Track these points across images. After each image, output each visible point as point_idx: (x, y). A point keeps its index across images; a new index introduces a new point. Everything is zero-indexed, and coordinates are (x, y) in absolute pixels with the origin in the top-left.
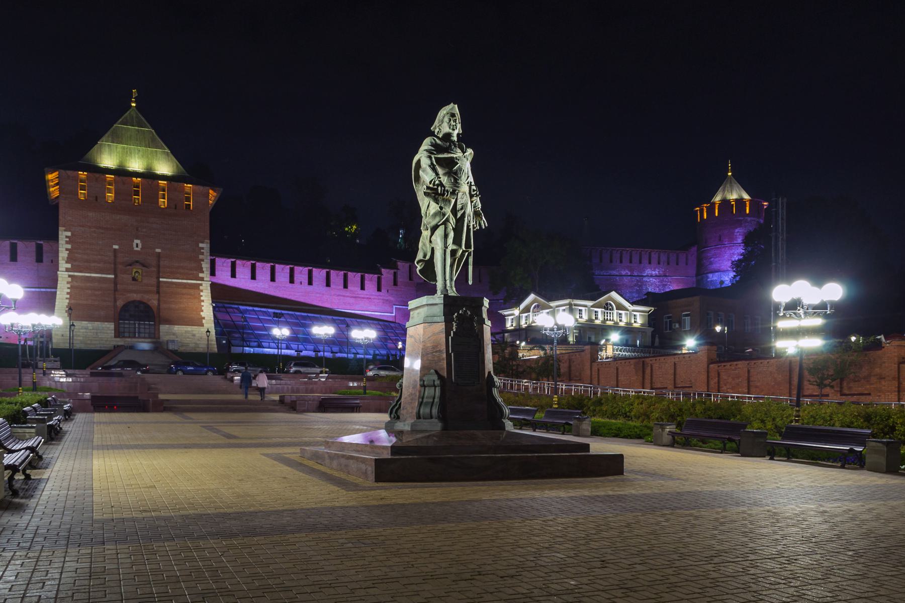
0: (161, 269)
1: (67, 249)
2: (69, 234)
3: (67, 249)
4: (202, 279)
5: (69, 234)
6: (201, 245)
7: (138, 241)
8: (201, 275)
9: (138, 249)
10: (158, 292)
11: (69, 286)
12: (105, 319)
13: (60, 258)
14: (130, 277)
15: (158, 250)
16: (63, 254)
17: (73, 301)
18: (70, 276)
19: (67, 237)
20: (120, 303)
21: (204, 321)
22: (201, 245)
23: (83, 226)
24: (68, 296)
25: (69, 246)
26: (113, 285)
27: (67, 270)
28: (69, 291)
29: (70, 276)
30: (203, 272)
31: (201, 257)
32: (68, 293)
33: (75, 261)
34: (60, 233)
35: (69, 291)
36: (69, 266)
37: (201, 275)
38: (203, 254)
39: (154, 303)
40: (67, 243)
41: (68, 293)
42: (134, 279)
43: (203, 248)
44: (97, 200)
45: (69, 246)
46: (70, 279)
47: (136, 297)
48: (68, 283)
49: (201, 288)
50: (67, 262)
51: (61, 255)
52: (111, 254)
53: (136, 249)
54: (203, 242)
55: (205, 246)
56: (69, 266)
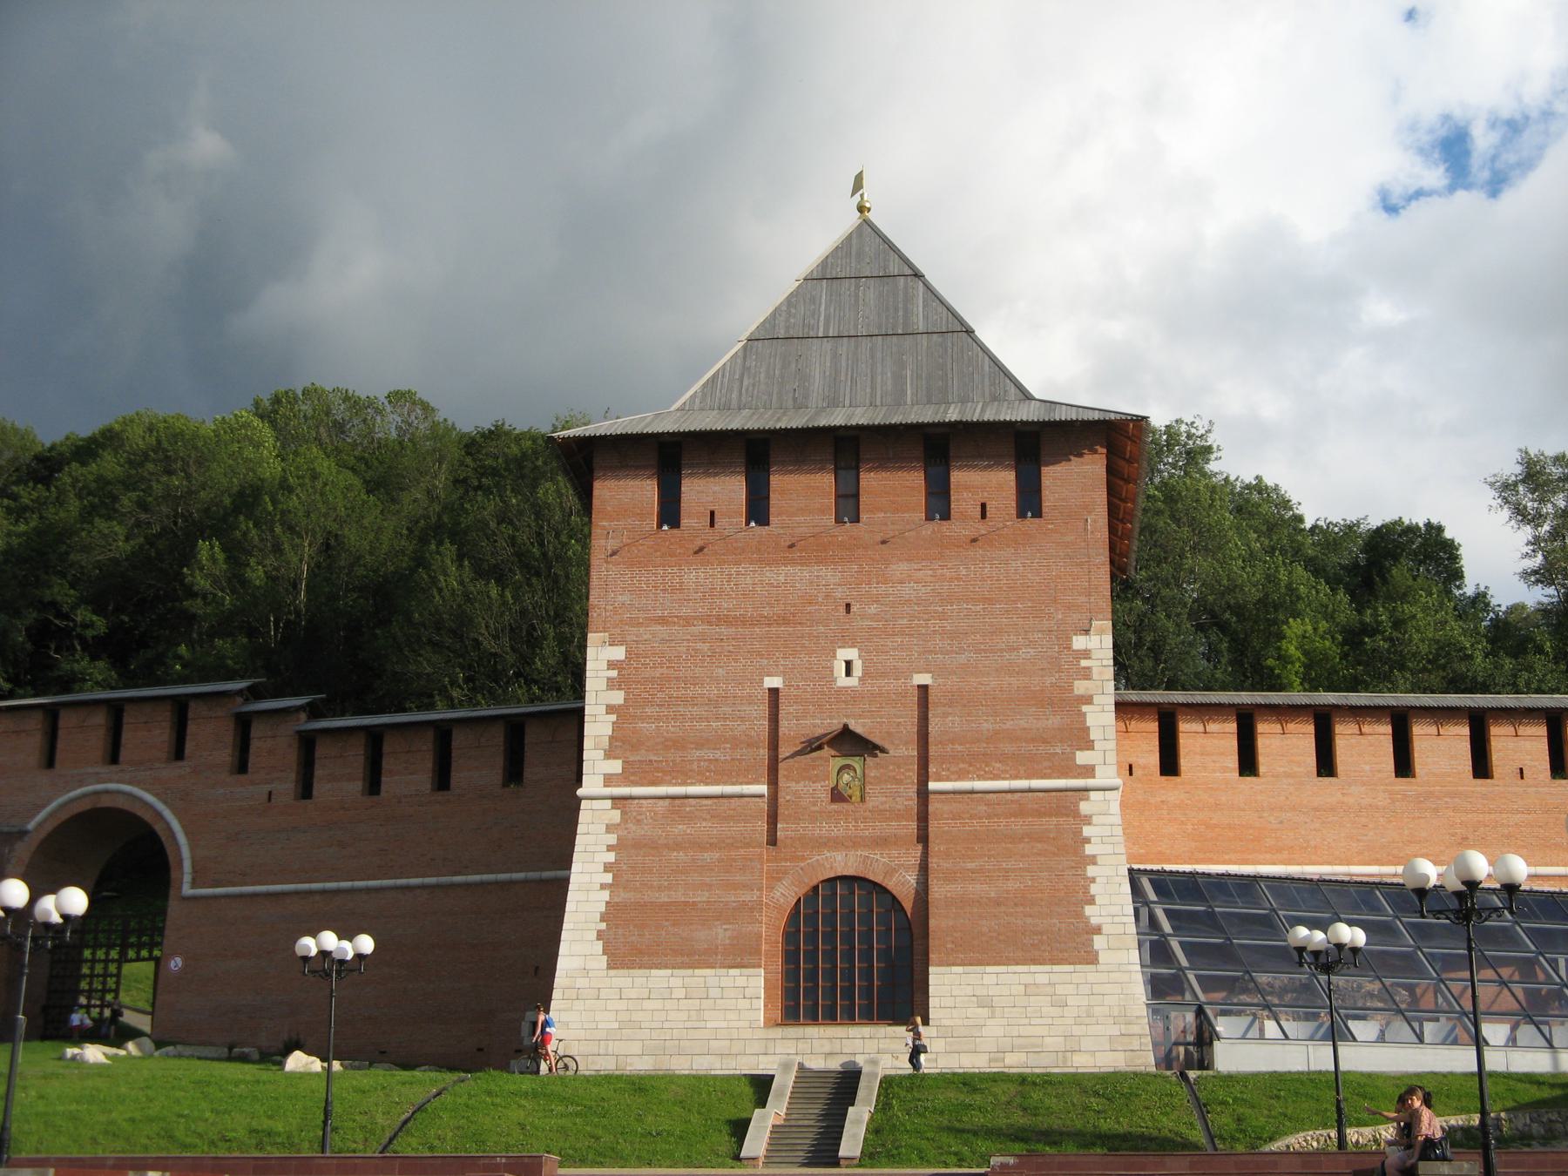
0: (933, 750)
1: (610, 709)
2: (619, 653)
3: (610, 709)
4: (1089, 771)
5: (619, 653)
6: (1079, 642)
7: (852, 653)
8: (1082, 757)
9: (853, 682)
10: (923, 838)
11: (612, 839)
12: (738, 955)
13: (587, 744)
14: (821, 790)
15: (923, 679)
16: (598, 727)
17: (623, 896)
18: (617, 800)
19: (612, 665)
20: (786, 894)
21: (1099, 942)
22: (1079, 642)
23: (662, 621)
24: (608, 878)
25: (618, 697)
26: (763, 826)
27: (609, 780)
28: (611, 857)
29: (617, 800)
30: (1089, 745)
31: (1080, 687)
32: (608, 868)
33: (635, 747)
34: (591, 652)
35: (611, 857)
36: (616, 766)
37: (1082, 757)
38: (1086, 674)
39: (903, 884)
40: (612, 684)
41: (608, 868)
42: (837, 796)
43: (1086, 654)
44: (712, 525)
45: (618, 697)
46: (616, 816)
47: (843, 863)
48: (610, 829)
49: (1084, 807)
50: (609, 755)
51: (589, 729)
52: (764, 709)
53: (842, 681)
54: (1087, 632)
55: (1098, 645)
56: (616, 766)
